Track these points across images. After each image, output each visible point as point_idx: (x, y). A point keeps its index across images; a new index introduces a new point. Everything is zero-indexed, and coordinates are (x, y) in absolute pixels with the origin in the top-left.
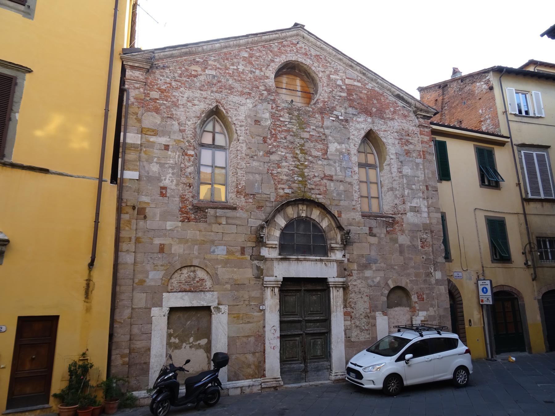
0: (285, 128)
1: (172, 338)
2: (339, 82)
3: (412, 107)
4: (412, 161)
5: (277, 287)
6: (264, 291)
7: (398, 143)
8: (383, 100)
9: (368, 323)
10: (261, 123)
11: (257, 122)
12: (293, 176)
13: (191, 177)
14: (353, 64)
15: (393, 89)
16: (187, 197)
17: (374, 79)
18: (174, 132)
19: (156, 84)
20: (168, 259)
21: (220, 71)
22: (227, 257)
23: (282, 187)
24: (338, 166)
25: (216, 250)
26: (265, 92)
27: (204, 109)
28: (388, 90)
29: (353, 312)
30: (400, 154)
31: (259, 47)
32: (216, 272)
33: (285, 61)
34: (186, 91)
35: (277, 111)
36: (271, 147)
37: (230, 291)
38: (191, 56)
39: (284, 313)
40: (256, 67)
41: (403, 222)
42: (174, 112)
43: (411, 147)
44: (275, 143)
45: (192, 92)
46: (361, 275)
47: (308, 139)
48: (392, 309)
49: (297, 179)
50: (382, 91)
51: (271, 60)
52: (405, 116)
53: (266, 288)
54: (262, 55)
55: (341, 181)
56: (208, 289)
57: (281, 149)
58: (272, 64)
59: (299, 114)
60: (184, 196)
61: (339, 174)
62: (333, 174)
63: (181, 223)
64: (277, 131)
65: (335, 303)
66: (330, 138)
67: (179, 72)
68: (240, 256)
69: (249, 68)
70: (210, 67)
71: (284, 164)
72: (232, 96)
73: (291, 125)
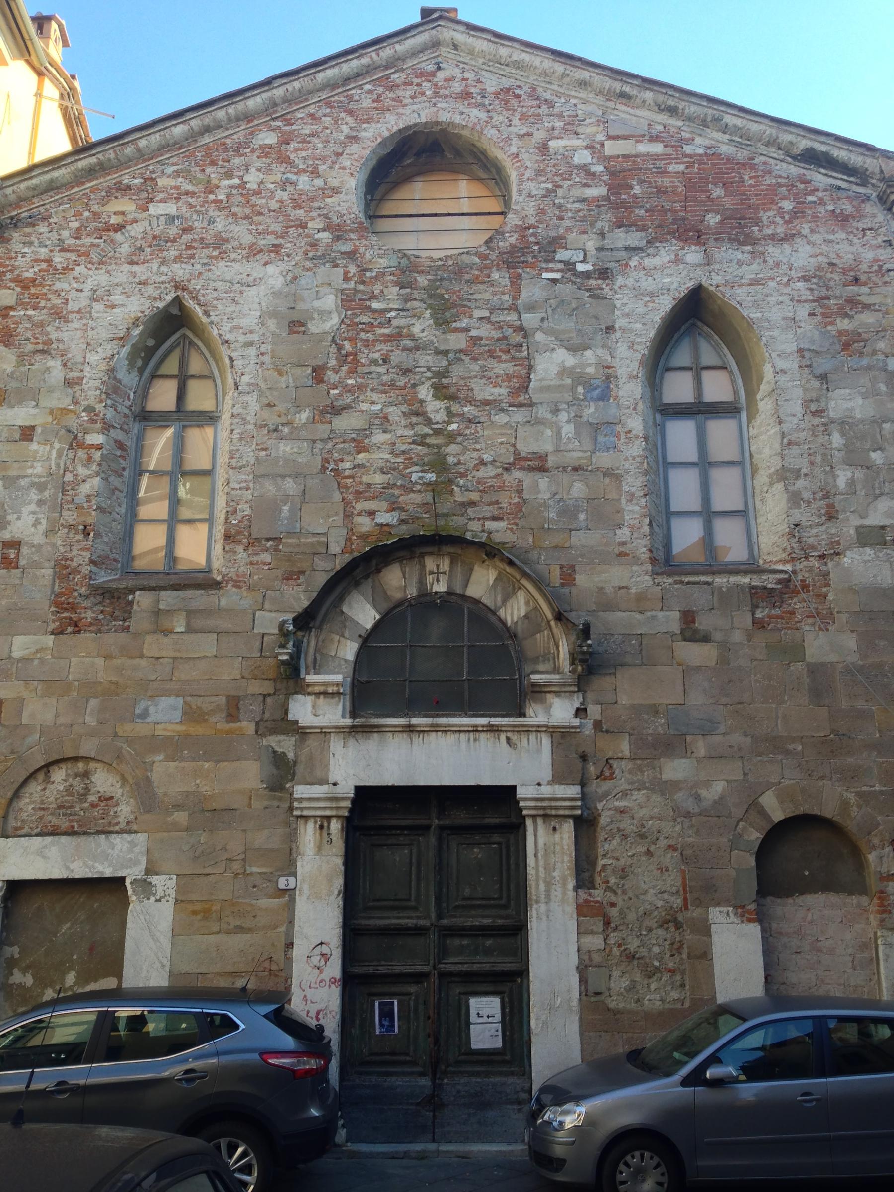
0: (387, 331)
1: (16, 971)
2: (583, 157)
3: (874, 181)
4: (869, 368)
5: (338, 816)
6: (296, 829)
7: (812, 314)
8: (752, 182)
9: (676, 948)
10: (309, 325)
11: (296, 326)
12: (408, 471)
13: (90, 507)
14: (627, 89)
15: (786, 137)
16: (74, 564)
17: (709, 119)
18: (51, 390)
19: (10, 268)
20: (10, 741)
21: (191, 200)
22: (182, 728)
23: (367, 509)
24: (569, 421)
25: (152, 710)
26: (325, 236)
27: (139, 315)
28: (768, 144)
29: (613, 905)
30: (816, 352)
31: (312, 109)
32: (149, 774)
33: (395, 129)
34: (91, 272)
35: (363, 282)
36: (336, 392)
37: (187, 829)
38: (109, 174)
39: (371, 904)
40: (301, 167)
41: (828, 585)
42: (54, 336)
43: (868, 318)
44: (350, 378)
45: (108, 272)
46: (648, 775)
47: (461, 351)
48: (790, 901)
49: (421, 478)
50: (745, 153)
51: (348, 137)
52: (843, 219)
53: (301, 822)
54: (320, 130)
55: (575, 469)
56: (123, 825)
57: (369, 393)
58: (354, 148)
59: (437, 280)
60: (68, 562)
61: (571, 447)
62: (548, 447)
63: (53, 637)
64: (359, 344)
65: (541, 869)
66: (539, 336)
67: (75, 225)
68: (224, 726)
69: (278, 173)
70: (161, 196)
71: (379, 437)
72: (222, 264)
73: (406, 317)
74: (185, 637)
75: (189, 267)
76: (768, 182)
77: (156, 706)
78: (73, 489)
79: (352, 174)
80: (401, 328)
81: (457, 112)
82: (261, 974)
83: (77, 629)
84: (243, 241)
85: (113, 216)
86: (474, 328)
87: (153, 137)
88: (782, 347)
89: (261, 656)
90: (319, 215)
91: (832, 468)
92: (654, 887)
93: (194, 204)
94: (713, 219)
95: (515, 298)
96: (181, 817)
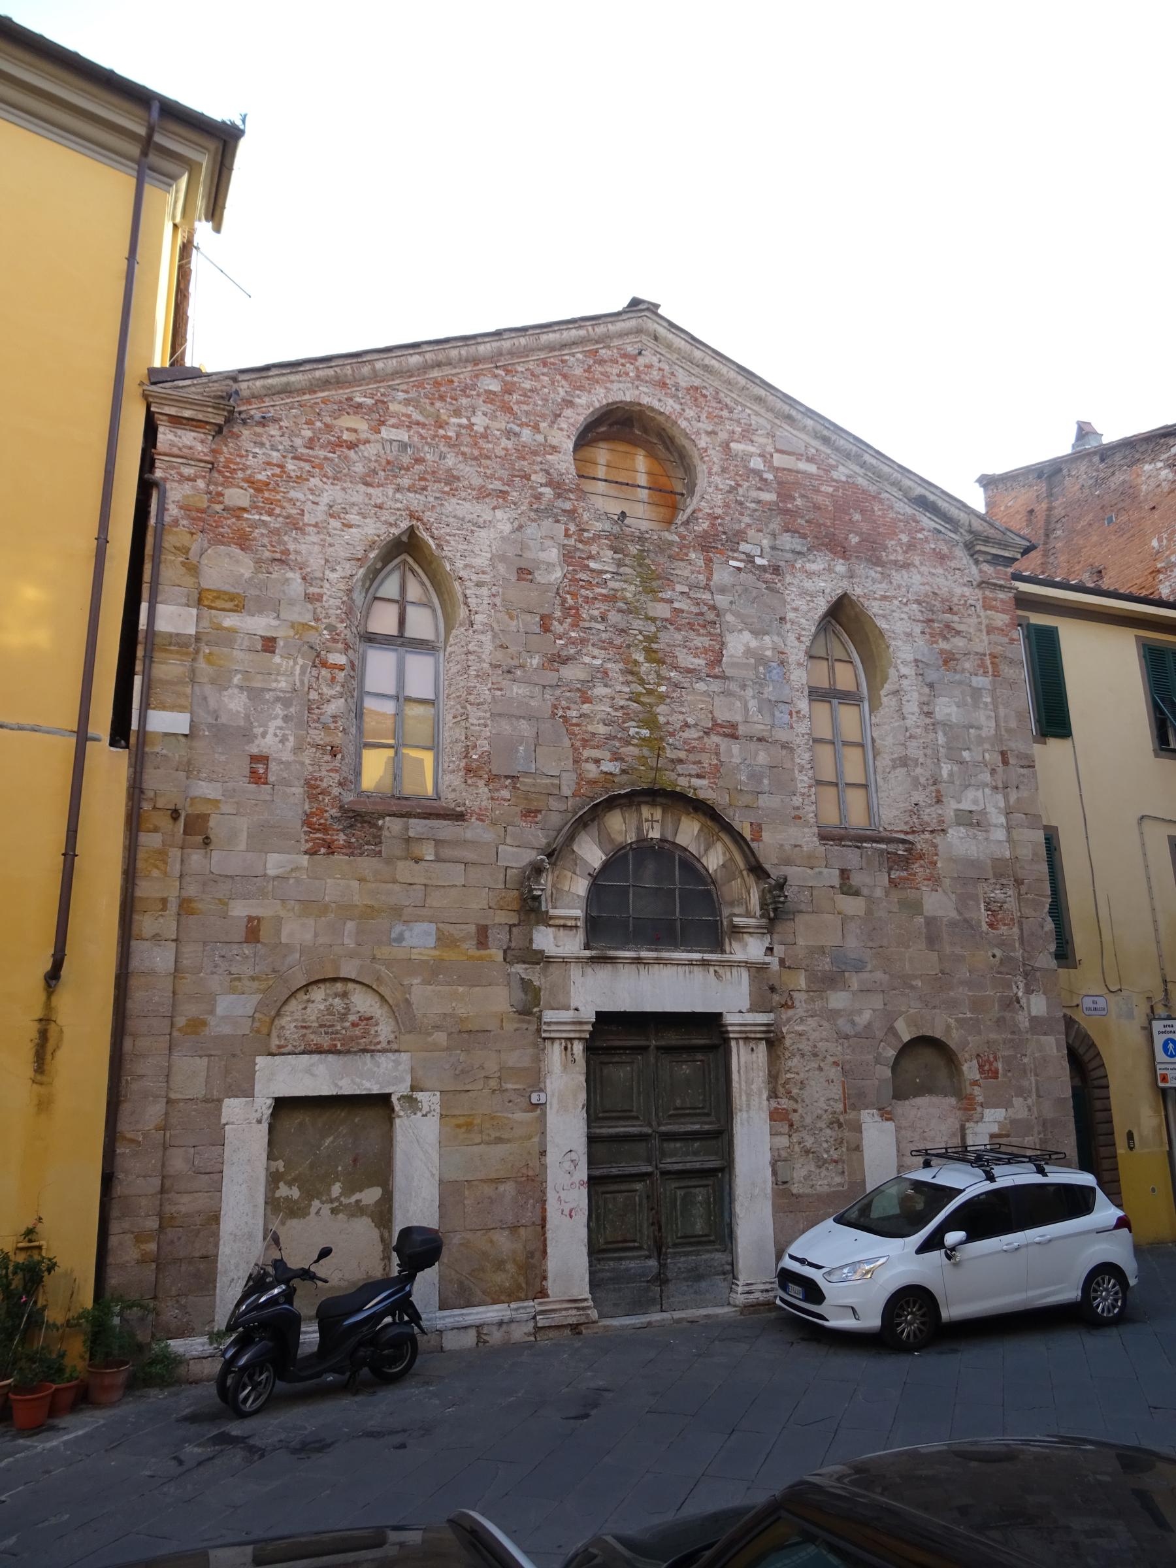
0: (604, 591)
1: (281, 1184)
2: (756, 463)
3: (962, 530)
4: (960, 683)
5: (580, 1039)
6: (544, 1049)
7: (923, 633)
8: (880, 513)
9: (839, 1142)
10: (536, 574)
11: (524, 573)
12: (626, 725)
13: (336, 728)
14: (793, 413)
15: (907, 483)
16: (324, 785)
17: (853, 453)
18: (292, 603)
19: (241, 466)
20: (270, 960)
21: (422, 431)
22: (437, 953)
23: (593, 756)
24: (753, 697)
25: (407, 934)
26: (547, 491)
27: (376, 538)
28: (893, 484)
29: (795, 1111)
30: (927, 664)
31: (531, 366)
32: (408, 996)
33: (605, 402)
34: (326, 486)
35: (581, 541)
36: (562, 642)
37: (448, 1049)
38: (341, 388)
39: (601, 1115)
40: (523, 420)
41: (937, 855)
42: (291, 547)
43: (959, 642)
44: (574, 631)
45: (344, 489)
46: (818, 1005)
47: (666, 620)
48: (907, 1102)
49: (637, 733)
50: (875, 488)
51: (563, 400)
52: (942, 558)
53: (548, 1043)
54: (539, 387)
55: (760, 740)
56: (384, 1045)
57: (590, 648)
58: (568, 412)
59: (644, 551)
60: (318, 783)
61: (755, 719)
62: (738, 718)
63: (307, 857)
64: (580, 600)
65: (743, 1083)
66: (729, 618)
67: (308, 433)
68: (474, 952)
69: (502, 422)
70: (392, 421)
71: (600, 690)
72: (454, 500)
73: (620, 581)
74: (433, 865)
75: (422, 498)
76: (891, 516)
77: (411, 930)
78: (318, 708)
79: (569, 437)
80: (616, 590)
81: (656, 398)
82: (519, 1179)
83: (331, 851)
84: (473, 482)
85: (345, 432)
86: (677, 600)
87: (390, 361)
88: (904, 656)
89: (506, 888)
90: (541, 470)
91: (938, 760)
92: (823, 1095)
93: (425, 435)
94: (854, 539)
95: (709, 579)
96: (441, 1038)
